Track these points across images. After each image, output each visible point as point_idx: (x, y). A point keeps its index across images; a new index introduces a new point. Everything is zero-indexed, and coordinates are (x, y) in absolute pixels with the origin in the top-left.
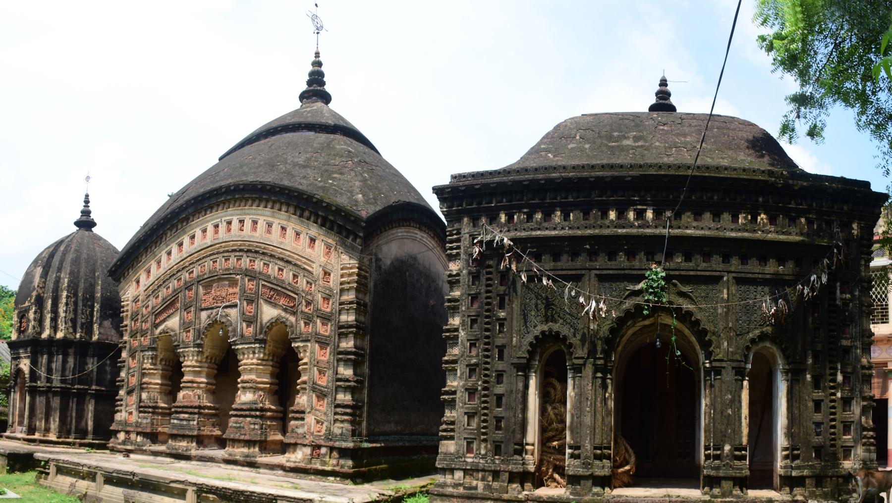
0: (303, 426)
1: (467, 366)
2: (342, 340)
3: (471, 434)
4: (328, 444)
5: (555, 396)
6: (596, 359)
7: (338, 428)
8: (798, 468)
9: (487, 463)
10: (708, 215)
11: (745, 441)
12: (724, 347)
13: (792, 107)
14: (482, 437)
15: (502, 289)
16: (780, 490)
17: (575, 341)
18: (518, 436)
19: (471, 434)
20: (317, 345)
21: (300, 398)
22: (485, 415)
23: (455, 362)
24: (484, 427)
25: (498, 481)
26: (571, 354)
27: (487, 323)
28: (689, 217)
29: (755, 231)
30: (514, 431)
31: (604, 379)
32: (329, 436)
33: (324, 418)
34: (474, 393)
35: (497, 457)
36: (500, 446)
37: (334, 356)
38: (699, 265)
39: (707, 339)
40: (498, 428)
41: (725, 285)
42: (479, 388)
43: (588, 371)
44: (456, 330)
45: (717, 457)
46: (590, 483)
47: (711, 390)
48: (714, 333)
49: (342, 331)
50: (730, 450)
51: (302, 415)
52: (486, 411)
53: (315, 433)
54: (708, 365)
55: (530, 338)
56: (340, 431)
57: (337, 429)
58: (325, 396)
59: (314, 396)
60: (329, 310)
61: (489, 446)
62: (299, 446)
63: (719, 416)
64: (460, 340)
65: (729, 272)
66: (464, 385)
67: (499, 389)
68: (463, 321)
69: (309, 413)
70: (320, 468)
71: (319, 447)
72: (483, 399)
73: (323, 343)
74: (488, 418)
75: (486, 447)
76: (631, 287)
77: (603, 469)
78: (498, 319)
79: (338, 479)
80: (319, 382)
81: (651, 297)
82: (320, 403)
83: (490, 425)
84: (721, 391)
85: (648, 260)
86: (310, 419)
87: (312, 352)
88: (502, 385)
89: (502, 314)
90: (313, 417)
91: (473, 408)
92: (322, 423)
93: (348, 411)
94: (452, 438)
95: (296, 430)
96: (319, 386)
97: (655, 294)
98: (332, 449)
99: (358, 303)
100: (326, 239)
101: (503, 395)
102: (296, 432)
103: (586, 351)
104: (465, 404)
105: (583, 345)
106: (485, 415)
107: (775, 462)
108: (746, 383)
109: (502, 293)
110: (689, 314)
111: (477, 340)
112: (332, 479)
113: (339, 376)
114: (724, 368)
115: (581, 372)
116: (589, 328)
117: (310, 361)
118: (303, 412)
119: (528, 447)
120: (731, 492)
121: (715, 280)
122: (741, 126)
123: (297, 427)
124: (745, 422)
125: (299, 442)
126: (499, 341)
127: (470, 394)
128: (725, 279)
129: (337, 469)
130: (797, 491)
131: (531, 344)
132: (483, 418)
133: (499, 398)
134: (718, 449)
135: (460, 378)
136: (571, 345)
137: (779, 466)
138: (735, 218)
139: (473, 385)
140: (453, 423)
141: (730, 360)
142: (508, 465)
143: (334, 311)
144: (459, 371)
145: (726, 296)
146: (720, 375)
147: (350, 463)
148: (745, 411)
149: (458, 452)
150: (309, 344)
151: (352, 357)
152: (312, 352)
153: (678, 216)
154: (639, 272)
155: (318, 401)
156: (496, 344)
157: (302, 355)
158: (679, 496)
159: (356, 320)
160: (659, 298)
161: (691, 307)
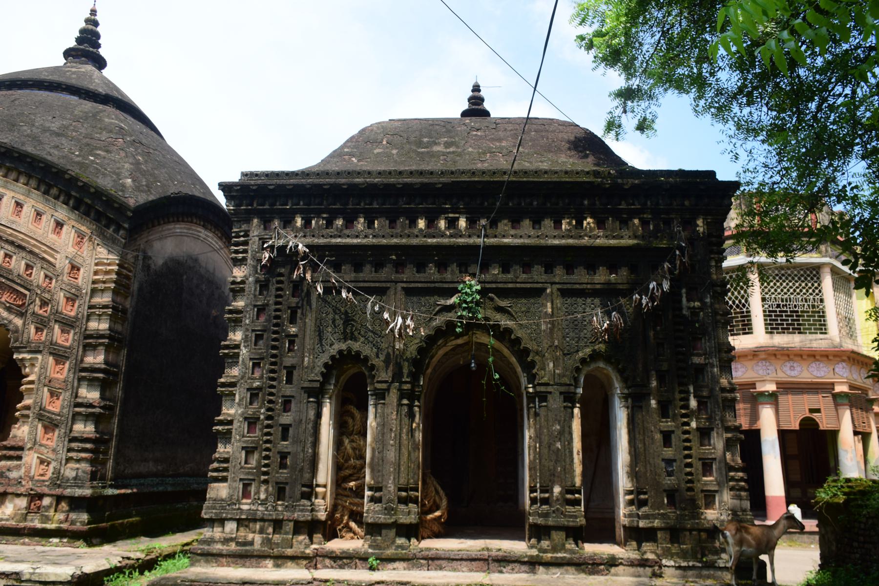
0: (18, 467)
1: (248, 390)
2: (88, 353)
3: (248, 473)
4: (53, 492)
5: (354, 426)
6: (401, 383)
7: (72, 469)
8: (646, 517)
9: (267, 510)
10: (527, 223)
11: (578, 481)
12: (549, 369)
13: (617, 102)
14: (263, 478)
15: (294, 300)
16: (625, 545)
17: (378, 362)
18: (307, 476)
19: (248, 473)
20: (51, 358)
21: (19, 428)
22: (267, 449)
23: (233, 385)
24: (266, 466)
25: (280, 533)
26: (374, 377)
27: (275, 340)
28: (506, 225)
29: (581, 237)
30: (302, 470)
32: (58, 480)
33: (51, 456)
34: (255, 423)
35: (279, 503)
36: (284, 488)
37: (74, 373)
38: (518, 277)
39: (529, 359)
40: (283, 466)
41: (549, 298)
42: (262, 417)
43: (393, 397)
44: (237, 346)
45: (545, 501)
46: (393, 532)
47: (535, 420)
48: (537, 353)
49: (89, 342)
50: (561, 493)
51: (19, 453)
52: (268, 445)
53: (36, 478)
54: (531, 390)
55: (325, 358)
56: (74, 474)
57: (69, 472)
58: (57, 426)
59: (40, 426)
60: (73, 314)
61: (271, 489)
62: (10, 497)
63: (546, 451)
64: (241, 359)
65: (552, 283)
66: (243, 413)
67: (286, 419)
68: (246, 336)
69: (29, 449)
70: (39, 526)
71: (41, 496)
72: (266, 430)
73: (60, 356)
74: (271, 454)
75: (267, 490)
76: (442, 302)
77: (408, 515)
78: (288, 336)
79: (65, 540)
80: (50, 408)
81: (464, 313)
82: (47, 436)
83: (273, 462)
84: (547, 421)
85: (461, 272)
86: (31, 458)
87: (43, 367)
88: (289, 414)
89: (293, 330)
90: (36, 455)
91: (253, 442)
92: (49, 464)
93: (88, 446)
94: (224, 480)
95: (8, 473)
96: (49, 412)
97: (469, 309)
98: (59, 499)
99: (113, 308)
100: (77, 225)
101: (290, 425)
102: (7, 477)
103: (390, 374)
104: (243, 436)
105: (387, 367)
106: (267, 449)
107: (617, 509)
108: (576, 411)
109: (294, 305)
110: (508, 331)
111: (262, 359)
112: (55, 540)
113: (79, 400)
114: (550, 393)
115: (384, 399)
116: (394, 347)
117: (39, 379)
118: (21, 449)
119: (319, 490)
121: (537, 293)
122: (561, 127)
123: (9, 470)
124: (577, 459)
125: (10, 490)
126: (288, 361)
127: (249, 424)
128: (548, 291)
129: (64, 526)
130: (647, 546)
131: (326, 365)
132: (264, 453)
133: (286, 428)
134: (546, 491)
135: (239, 404)
136: (373, 367)
137: (622, 514)
138: (558, 224)
139: (254, 413)
140: (226, 460)
141: (557, 384)
142: (294, 512)
143: (79, 316)
144: (237, 396)
145: (550, 310)
146: (546, 401)
147: (85, 517)
148: (577, 444)
149: (231, 497)
150: (40, 357)
151: (101, 375)
152: (43, 367)
153: (494, 224)
154: (451, 286)
155: (46, 433)
156: (284, 364)
157: (27, 370)
158: (500, 550)
159: (110, 329)
160: (474, 313)
161: (510, 323)
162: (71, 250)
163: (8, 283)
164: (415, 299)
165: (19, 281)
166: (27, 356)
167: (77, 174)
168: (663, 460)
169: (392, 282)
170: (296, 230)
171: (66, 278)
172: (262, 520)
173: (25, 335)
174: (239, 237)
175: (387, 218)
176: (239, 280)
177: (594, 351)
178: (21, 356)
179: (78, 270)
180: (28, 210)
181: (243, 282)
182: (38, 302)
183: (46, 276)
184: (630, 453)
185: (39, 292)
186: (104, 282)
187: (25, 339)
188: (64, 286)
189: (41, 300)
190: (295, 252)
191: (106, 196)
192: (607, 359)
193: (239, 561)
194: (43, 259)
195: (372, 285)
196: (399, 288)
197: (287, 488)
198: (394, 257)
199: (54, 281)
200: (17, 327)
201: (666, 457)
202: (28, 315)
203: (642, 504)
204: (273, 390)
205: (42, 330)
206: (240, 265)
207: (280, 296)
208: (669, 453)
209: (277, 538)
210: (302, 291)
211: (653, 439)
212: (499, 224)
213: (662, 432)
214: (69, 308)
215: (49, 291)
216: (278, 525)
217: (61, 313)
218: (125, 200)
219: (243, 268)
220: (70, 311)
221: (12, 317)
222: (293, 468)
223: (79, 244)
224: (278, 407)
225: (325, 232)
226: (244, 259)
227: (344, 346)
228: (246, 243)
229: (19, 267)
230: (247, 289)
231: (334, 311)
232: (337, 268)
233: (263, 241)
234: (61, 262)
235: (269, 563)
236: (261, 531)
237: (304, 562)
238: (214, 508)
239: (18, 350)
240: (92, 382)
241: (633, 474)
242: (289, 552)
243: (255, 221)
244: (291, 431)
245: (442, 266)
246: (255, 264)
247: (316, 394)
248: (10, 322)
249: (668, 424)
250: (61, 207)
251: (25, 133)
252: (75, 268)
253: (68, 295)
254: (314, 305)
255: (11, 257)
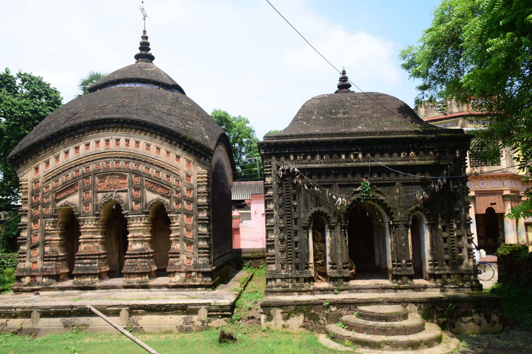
0: (178, 261)
1: (279, 228)
2: (199, 212)
3: (283, 261)
4: (196, 270)
6: (341, 223)
7: (201, 260)
9: (292, 274)
11: (411, 258)
12: (399, 215)
14: (289, 262)
15: (294, 191)
17: (331, 215)
18: (307, 260)
19: (283, 261)
20: (185, 216)
21: (175, 245)
22: (290, 251)
23: (273, 226)
24: (290, 257)
25: (298, 282)
26: (329, 221)
27: (288, 208)
29: (409, 160)
30: (304, 258)
31: (344, 232)
32: (196, 265)
33: (192, 256)
34: (283, 241)
35: (297, 271)
36: (298, 266)
37: (196, 221)
38: (385, 178)
39: (391, 211)
40: (297, 257)
41: (398, 187)
42: (286, 239)
43: (338, 229)
44: (272, 211)
45: (399, 266)
46: (342, 280)
48: (394, 209)
49: (200, 208)
50: (405, 263)
51: (178, 255)
52: (290, 250)
53: (187, 265)
54: (391, 223)
55: (309, 214)
56: (202, 262)
57: (200, 261)
58: (192, 244)
59: (185, 244)
60: (191, 196)
61: (293, 266)
62: (177, 273)
63: (399, 247)
64: (274, 216)
65: (398, 180)
66: (278, 238)
67: (296, 239)
68: (276, 207)
69: (182, 253)
70: (192, 284)
71: (190, 272)
72: (288, 244)
73: (189, 214)
74: (292, 253)
75: (291, 267)
76: (354, 190)
77: (347, 273)
78: (294, 206)
79: (204, 289)
80: (187, 236)
81: (365, 194)
82: (188, 248)
83: (293, 256)
84: (399, 235)
85: (361, 177)
86: (183, 257)
87: (182, 220)
88: (297, 237)
89: (295, 204)
90: (185, 256)
91: (283, 248)
92: (191, 259)
93: (206, 251)
94: (274, 263)
95: (174, 264)
96: (188, 238)
97: (366, 192)
98: (198, 272)
99: (208, 193)
101: (298, 241)
102: (174, 265)
103: (336, 220)
104: (280, 246)
105: (335, 217)
106: (290, 251)
107: (424, 267)
108: (409, 231)
109: (295, 193)
110: (382, 201)
111: (283, 215)
112: (200, 289)
113: (200, 233)
114: (400, 225)
116: (337, 209)
117: (181, 225)
118: (179, 253)
119: (310, 265)
120: (407, 282)
121: (393, 184)
123: (174, 262)
124: (410, 249)
125: (177, 270)
126: (295, 216)
127: (281, 241)
128: (397, 184)
129: (203, 283)
131: (310, 217)
132: (289, 253)
133: (296, 243)
134: (399, 262)
135: (276, 234)
136: (329, 217)
138: (399, 155)
139: (283, 237)
140: (273, 256)
141: (402, 221)
142: (303, 274)
143: (194, 197)
144: (275, 231)
145: (398, 192)
146: (398, 228)
147: (210, 279)
148: (410, 244)
149: (277, 270)
150: (180, 215)
151: (207, 222)
152: (182, 220)
154: (358, 183)
155: (187, 246)
156: (293, 217)
157: (174, 221)
158: (382, 284)
159: (207, 202)
160: (368, 194)
161: (382, 198)
162: (185, 169)
163: (160, 184)
164: (343, 189)
165: (165, 183)
166: (175, 215)
167: (185, 135)
168: (444, 248)
169: (334, 182)
170: (292, 161)
171: (185, 181)
172: (291, 278)
173: (172, 206)
174: (267, 164)
175: (329, 155)
176: (269, 183)
177: (416, 207)
178: (171, 215)
179: (190, 177)
180: (163, 151)
181: (271, 184)
182: (175, 192)
183: (176, 180)
184: (431, 246)
185: (175, 188)
186: (202, 182)
187: (172, 208)
188: (185, 185)
189: (176, 191)
190: (294, 172)
191: (200, 145)
192: (421, 210)
193: (284, 293)
194: (174, 173)
195: (326, 184)
196: (337, 185)
197: (300, 266)
198: (334, 172)
199: (180, 182)
200: (167, 203)
201: (445, 247)
202: (172, 198)
203: (436, 265)
204: (290, 228)
205: (179, 204)
206: (269, 177)
207: (288, 190)
208: (445, 245)
209: (297, 284)
210: (297, 187)
211: (440, 241)
212: (375, 156)
213: (443, 238)
214: (189, 194)
215: (179, 187)
216: (298, 279)
217: (186, 196)
218: (209, 147)
219: (270, 178)
220: (190, 195)
221: (164, 199)
222: (301, 258)
223: (188, 165)
224: (293, 234)
225: (304, 161)
226: (270, 174)
227: (316, 209)
228: (270, 167)
229: (164, 177)
230: (273, 187)
231: (311, 195)
232: (310, 177)
233: (279, 167)
234: (183, 175)
235: (296, 294)
236: (291, 282)
237: (310, 293)
238: (271, 274)
239: (170, 213)
240: (203, 225)
241: (432, 254)
242: (303, 289)
243: (273, 158)
244: (299, 244)
245: (353, 175)
246: (275, 176)
247: (306, 228)
248: (164, 201)
249: (445, 234)
250: (178, 149)
251: (155, 115)
252: (188, 176)
253: (188, 188)
254: (303, 193)
255: (159, 172)
